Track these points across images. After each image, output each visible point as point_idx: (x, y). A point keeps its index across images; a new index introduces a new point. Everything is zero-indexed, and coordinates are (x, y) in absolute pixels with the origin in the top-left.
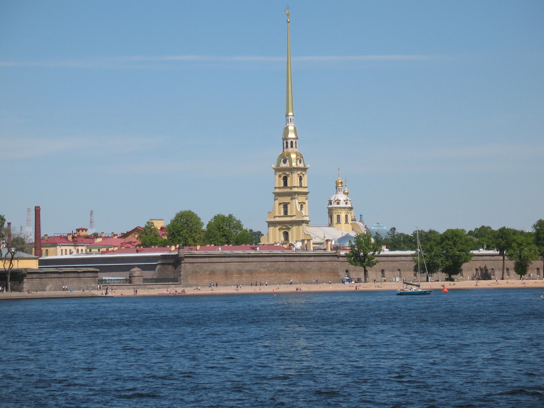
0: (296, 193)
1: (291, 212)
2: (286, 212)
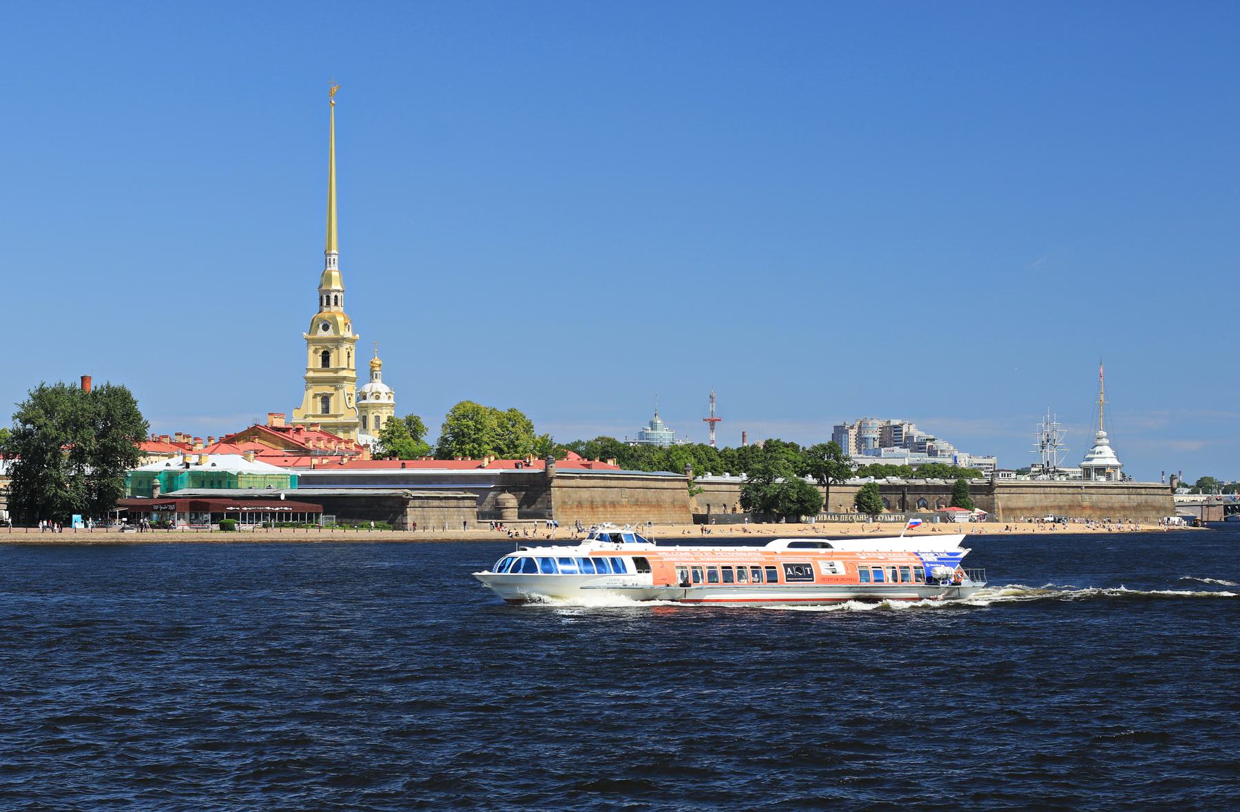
0: (344, 378)
1: (337, 408)
2: (326, 410)
